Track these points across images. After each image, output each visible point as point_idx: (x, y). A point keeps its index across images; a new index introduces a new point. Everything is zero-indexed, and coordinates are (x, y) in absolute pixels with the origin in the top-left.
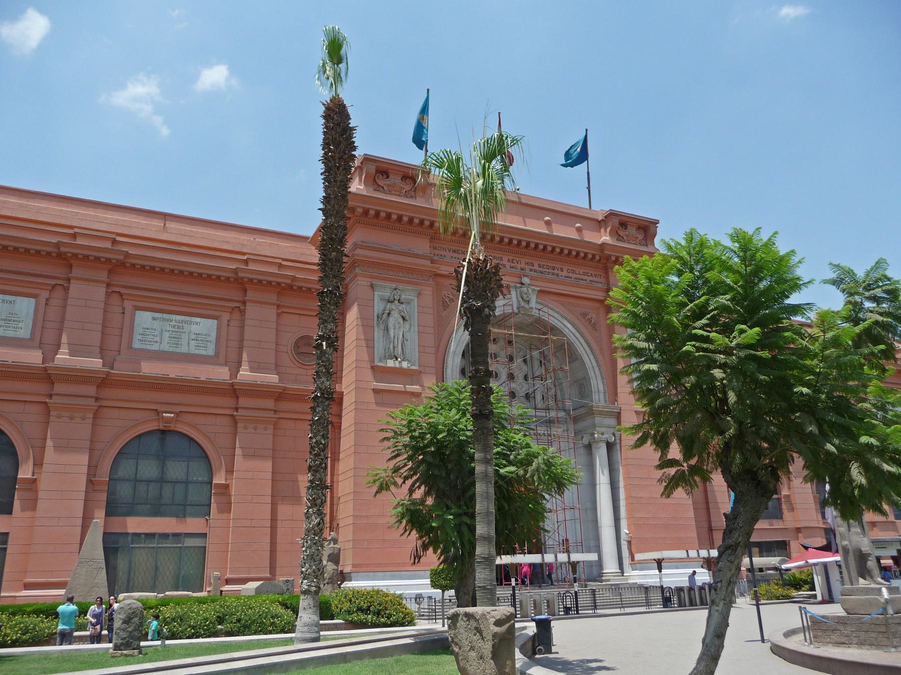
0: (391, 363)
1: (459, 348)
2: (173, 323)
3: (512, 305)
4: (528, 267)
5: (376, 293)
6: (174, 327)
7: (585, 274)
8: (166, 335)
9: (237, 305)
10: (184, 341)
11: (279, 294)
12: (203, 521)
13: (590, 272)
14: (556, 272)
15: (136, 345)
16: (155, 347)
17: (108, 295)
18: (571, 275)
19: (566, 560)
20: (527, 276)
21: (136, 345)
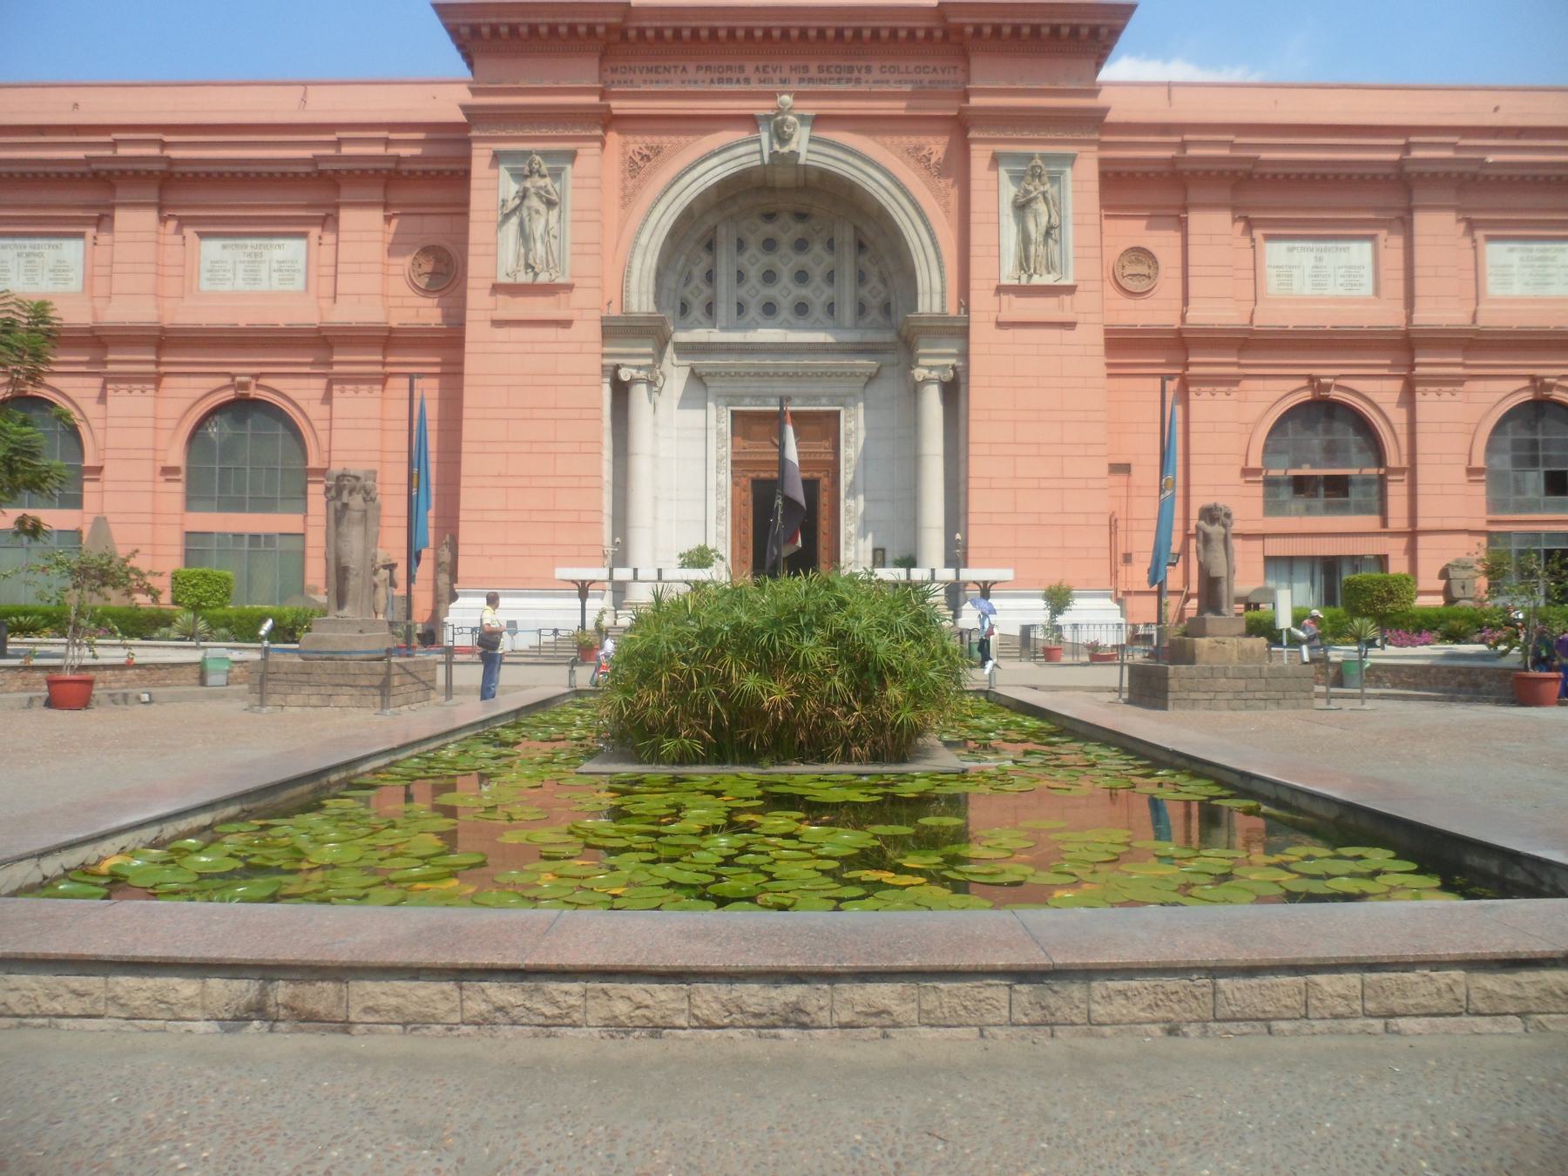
0: (524, 278)
1: (655, 239)
2: (249, 250)
3: (761, 152)
4: (795, 76)
5: (502, 168)
7: (918, 70)
8: (240, 267)
9: (330, 211)
10: (264, 275)
11: (386, 187)
12: (300, 517)
14: (856, 74)
15: (205, 286)
16: (227, 287)
17: (163, 220)
18: (887, 76)
19: (903, 578)
20: (789, 93)
21: (205, 286)
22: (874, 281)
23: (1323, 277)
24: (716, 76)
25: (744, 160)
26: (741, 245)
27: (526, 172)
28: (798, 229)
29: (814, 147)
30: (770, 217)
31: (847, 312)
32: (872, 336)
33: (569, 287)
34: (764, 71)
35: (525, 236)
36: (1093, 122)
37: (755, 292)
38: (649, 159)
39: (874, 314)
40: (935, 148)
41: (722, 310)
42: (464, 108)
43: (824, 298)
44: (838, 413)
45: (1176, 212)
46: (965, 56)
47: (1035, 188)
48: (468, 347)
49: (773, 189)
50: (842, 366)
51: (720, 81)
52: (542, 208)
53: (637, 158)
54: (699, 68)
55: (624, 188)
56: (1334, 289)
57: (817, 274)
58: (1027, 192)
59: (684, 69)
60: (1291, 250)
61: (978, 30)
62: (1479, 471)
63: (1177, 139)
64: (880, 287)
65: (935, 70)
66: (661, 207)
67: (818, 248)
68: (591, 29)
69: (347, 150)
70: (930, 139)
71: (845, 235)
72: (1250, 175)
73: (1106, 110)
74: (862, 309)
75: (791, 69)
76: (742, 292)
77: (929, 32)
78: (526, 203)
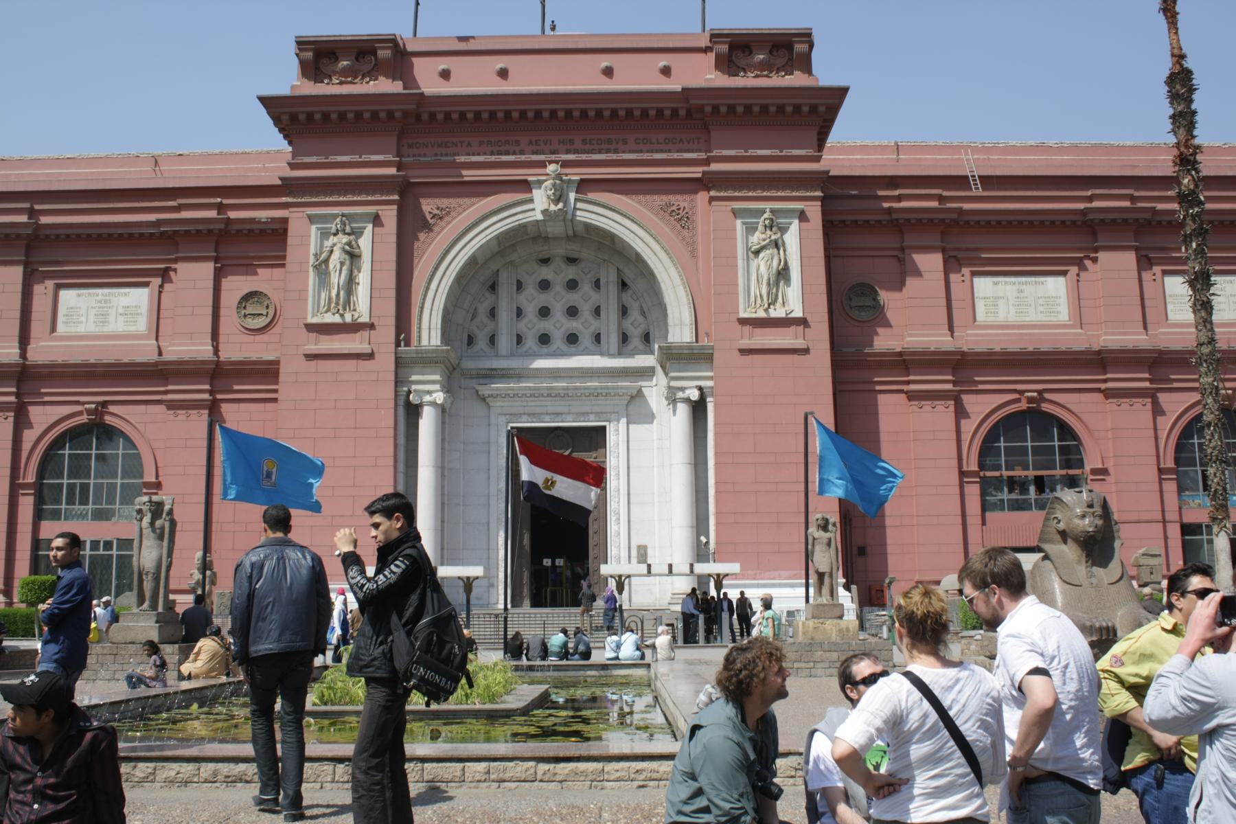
2: (100, 298)
6: (100, 302)
8: (94, 311)
10: (111, 318)
16: (81, 329)
20: (557, 162)
24: (495, 149)
27: (333, 230)
28: (571, 272)
29: (579, 205)
30: (545, 261)
31: (613, 340)
34: (537, 144)
37: (532, 325)
39: (636, 342)
40: (682, 205)
41: (505, 342)
42: (281, 179)
43: (592, 329)
44: (604, 428)
45: (895, 253)
46: (706, 129)
48: (282, 378)
50: (607, 388)
51: (500, 153)
52: (347, 257)
54: (481, 143)
56: (1033, 316)
57: (586, 310)
59: (469, 144)
60: (995, 284)
61: (716, 109)
62: (1168, 471)
64: (640, 319)
65: (681, 141)
67: (586, 287)
68: (390, 114)
69: (185, 215)
70: (678, 197)
71: (610, 278)
72: (956, 223)
74: (625, 338)
75: (560, 142)
76: (521, 326)
77: (675, 112)
78: (333, 257)
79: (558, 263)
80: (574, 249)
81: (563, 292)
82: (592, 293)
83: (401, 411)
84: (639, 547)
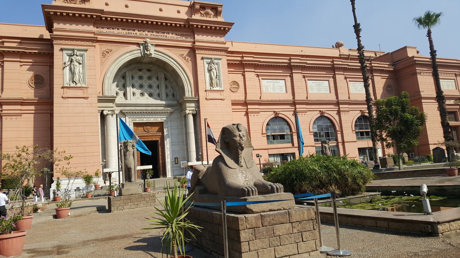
0: (73, 85)
13: (185, 34)
20: (149, 38)
22: (170, 88)
23: (274, 88)
24: (127, 32)
25: (136, 54)
26: (133, 78)
28: (148, 74)
29: (156, 52)
30: (140, 70)
31: (164, 96)
32: (171, 102)
33: (88, 88)
35: (72, 73)
36: (225, 50)
38: (108, 53)
39: (171, 97)
43: (157, 92)
47: (214, 66)
49: (142, 63)
53: (105, 52)
55: (102, 60)
56: (277, 91)
58: (211, 67)
63: (241, 55)
64: (172, 90)
66: (113, 66)
71: (162, 76)
73: (228, 48)
74: (167, 95)
77: (185, 25)
78: (72, 63)
79: (145, 71)
80: (150, 66)
81: (147, 80)
82: (156, 81)
83: (99, 117)
84: (175, 158)
